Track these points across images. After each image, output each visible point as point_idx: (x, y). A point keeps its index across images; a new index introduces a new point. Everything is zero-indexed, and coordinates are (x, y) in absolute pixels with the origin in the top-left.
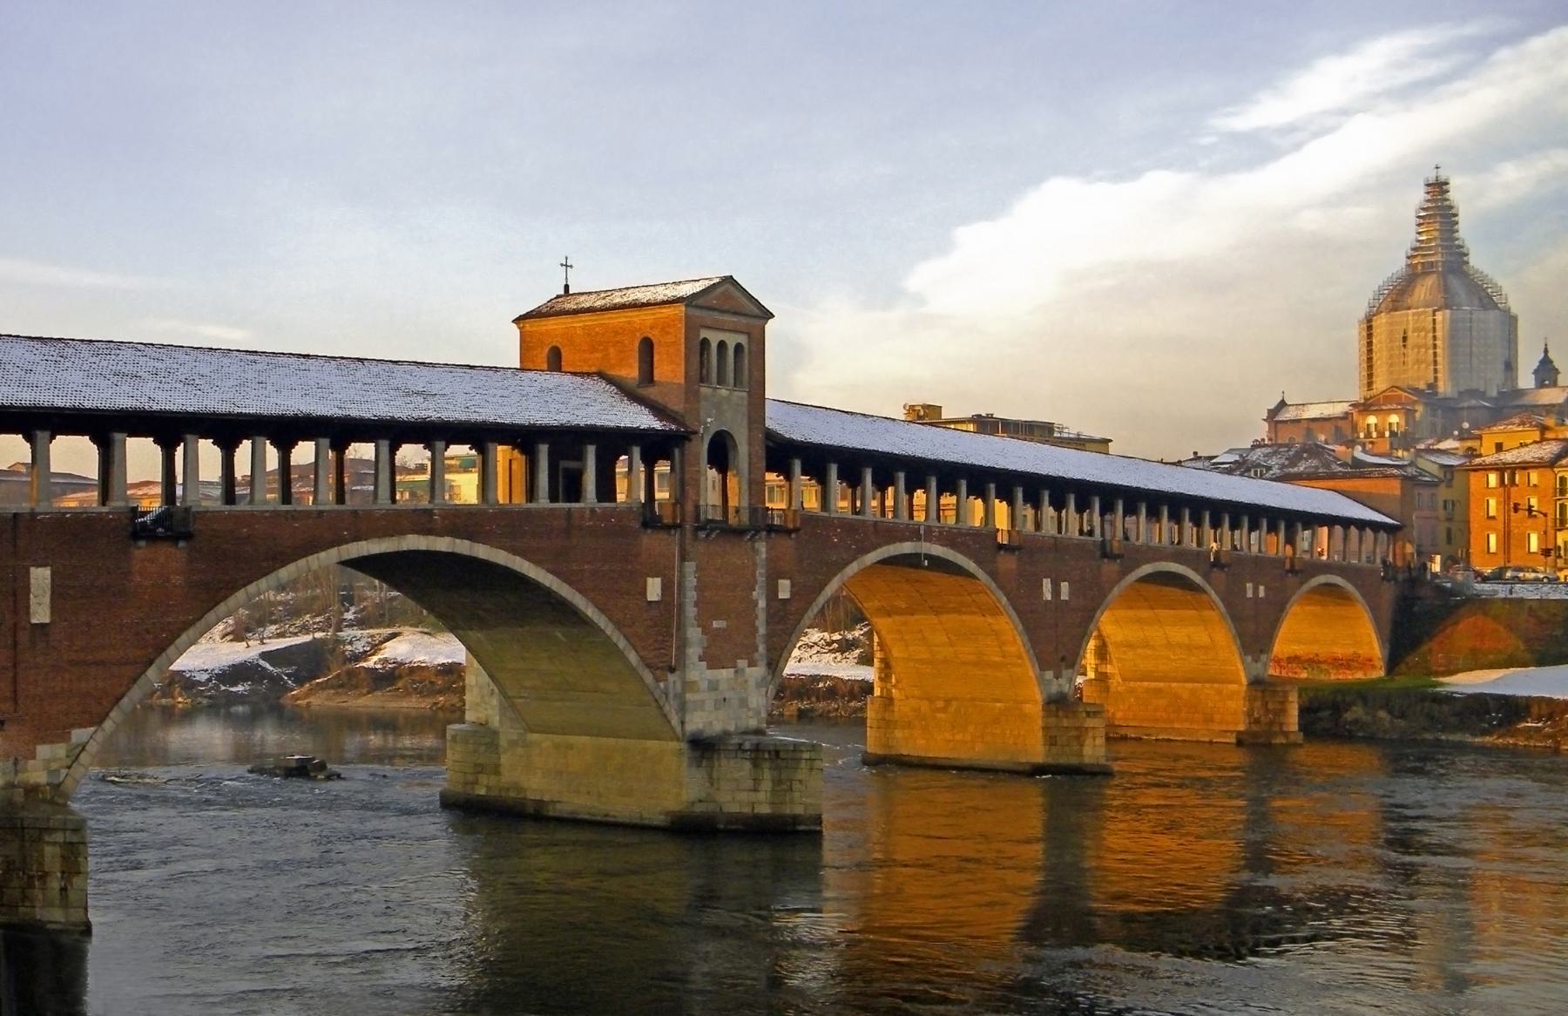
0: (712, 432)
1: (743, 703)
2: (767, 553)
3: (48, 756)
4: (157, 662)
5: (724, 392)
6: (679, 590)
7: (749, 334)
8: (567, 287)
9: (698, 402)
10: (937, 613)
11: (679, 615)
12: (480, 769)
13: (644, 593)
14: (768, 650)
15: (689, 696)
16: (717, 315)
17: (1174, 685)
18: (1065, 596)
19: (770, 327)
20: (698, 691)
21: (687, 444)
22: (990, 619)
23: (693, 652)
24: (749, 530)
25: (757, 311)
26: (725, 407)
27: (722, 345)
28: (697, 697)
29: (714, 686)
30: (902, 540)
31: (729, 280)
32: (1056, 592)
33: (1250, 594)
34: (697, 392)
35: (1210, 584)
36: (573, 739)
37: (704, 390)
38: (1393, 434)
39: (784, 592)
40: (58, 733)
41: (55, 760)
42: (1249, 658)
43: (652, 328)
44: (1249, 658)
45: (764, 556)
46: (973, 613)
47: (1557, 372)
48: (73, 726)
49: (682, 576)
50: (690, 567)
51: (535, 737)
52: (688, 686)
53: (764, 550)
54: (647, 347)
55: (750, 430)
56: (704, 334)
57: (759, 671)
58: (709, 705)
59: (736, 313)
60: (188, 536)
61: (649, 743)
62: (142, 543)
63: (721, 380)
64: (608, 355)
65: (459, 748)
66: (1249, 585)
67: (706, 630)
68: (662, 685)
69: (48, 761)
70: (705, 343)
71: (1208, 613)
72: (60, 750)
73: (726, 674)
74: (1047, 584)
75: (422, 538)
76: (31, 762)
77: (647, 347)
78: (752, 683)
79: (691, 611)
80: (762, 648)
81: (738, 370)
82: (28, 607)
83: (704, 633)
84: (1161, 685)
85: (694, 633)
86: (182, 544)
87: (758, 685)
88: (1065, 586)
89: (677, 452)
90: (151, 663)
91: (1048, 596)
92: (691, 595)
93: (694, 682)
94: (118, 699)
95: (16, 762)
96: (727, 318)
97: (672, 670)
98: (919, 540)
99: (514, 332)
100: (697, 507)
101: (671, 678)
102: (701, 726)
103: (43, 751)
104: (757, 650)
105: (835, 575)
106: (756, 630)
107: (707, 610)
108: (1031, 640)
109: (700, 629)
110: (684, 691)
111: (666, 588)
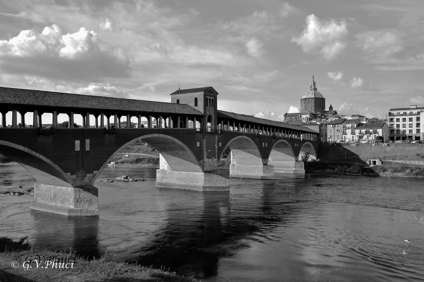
0: (208, 115)
1: (213, 165)
2: (218, 137)
3: (89, 176)
4: (110, 158)
5: (210, 108)
6: (203, 144)
7: (214, 97)
8: (179, 88)
9: (206, 109)
10: (244, 149)
11: (202, 149)
12: (163, 178)
13: (196, 145)
14: (218, 155)
15: (204, 164)
16: (209, 94)
17: (282, 162)
18: (266, 146)
19: (218, 96)
20: (206, 163)
21: (204, 117)
22: (254, 150)
23: (205, 156)
24: (214, 134)
25: (216, 93)
26: (210, 111)
27: (210, 99)
28: (206, 164)
29: (208, 162)
30: (240, 136)
31: (212, 87)
32: (265, 145)
33: (295, 145)
34: (206, 108)
35: (289, 143)
36: (181, 172)
37: (207, 107)
38: (308, 118)
39: (220, 145)
41: (90, 177)
42: (295, 157)
43: (197, 96)
44: (295, 157)
45: (217, 138)
46: (251, 149)
47: (333, 108)
48: (94, 170)
49: (203, 142)
50: (204, 140)
51: (174, 172)
52: (204, 162)
53: (217, 137)
54: (196, 99)
55: (215, 115)
56: (207, 97)
57: (216, 159)
58: (208, 166)
59: (212, 93)
60: (115, 134)
61: (196, 173)
62: (107, 135)
64: (188, 101)
65: (159, 174)
66: (295, 144)
67: (207, 152)
68: (200, 162)
69: (89, 177)
70: (207, 99)
71: (289, 149)
72: (91, 175)
73: (210, 160)
74: (263, 143)
75: (158, 134)
76: (86, 178)
77: (196, 99)
78: (215, 161)
79: (205, 148)
80: (217, 155)
81: (212, 104)
82: (85, 147)
83: (207, 152)
84: (279, 162)
85: (205, 152)
86: (114, 135)
87: (216, 162)
88: (266, 144)
89: (202, 119)
90: (108, 158)
91: (264, 146)
92: (205, 145)
93: (205, 162)
94: (102, 165)
95: (83, 178)
96: (211, 94)
97: (201, 159)
98: (243, 135)
99: (170, 97)
100: (206, 129)
101: (201, 161)
102: (206, 170)
103: (88, 175)
104: (216, 155)
105: (229, 142)
106: (216, 152)
107: (207, 148)
108: (261, 153)
110: (203, 163)
111: (200, 144)
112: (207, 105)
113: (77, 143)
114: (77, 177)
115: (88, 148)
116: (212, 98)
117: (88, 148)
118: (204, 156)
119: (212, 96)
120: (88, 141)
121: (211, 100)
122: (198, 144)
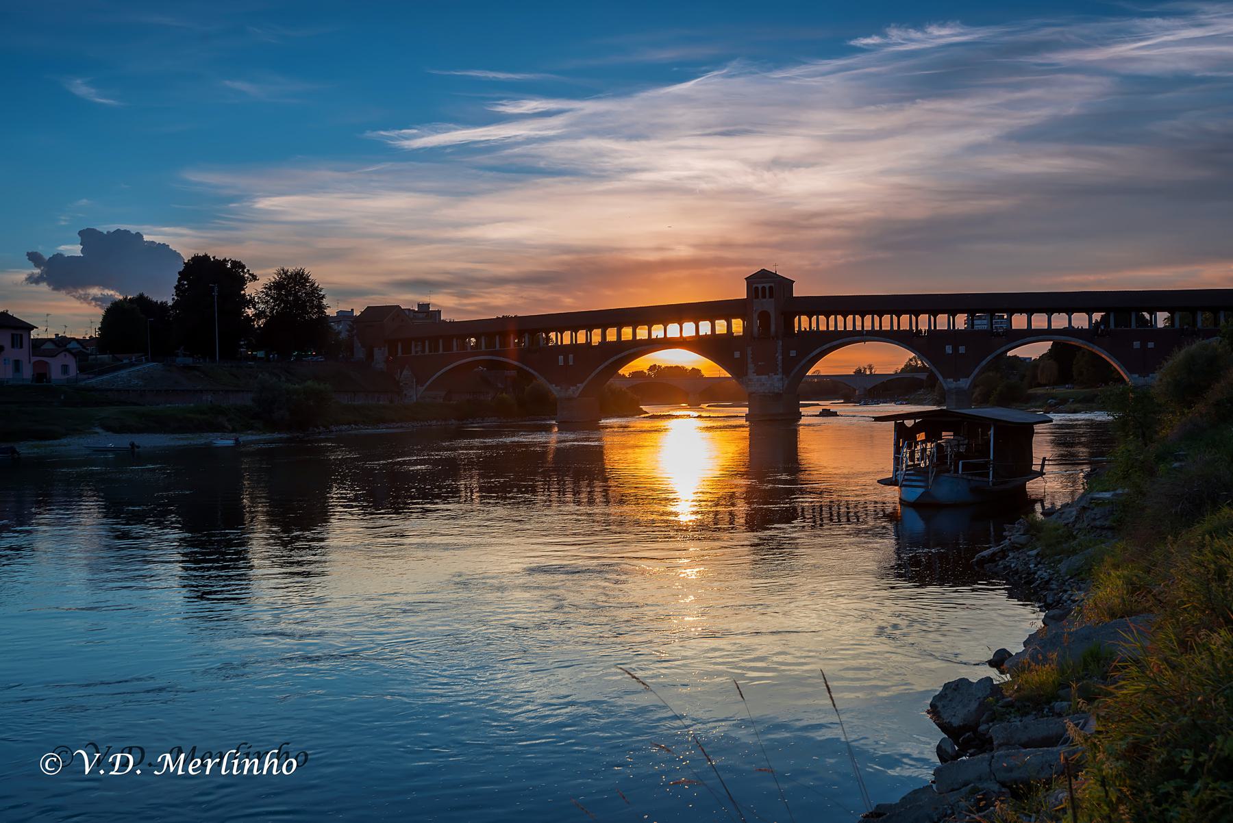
5: (764, 300)
27: (764, 288)
32: (955, 349)
45: (781, 344)
56: (756, 285)
57: (780, 376)
63: (764, 297)
72: (575, 388)
79: (750, 360)
80: (780, 370)
103: (572, 388)
109: (753, 365)
112: (757, 297)
113: (561, 358)
114: (561, 389)
115: (571, 363)
117: (571, 363)
120: (571, 356)
121: (760, 288)
122: (737, 355)
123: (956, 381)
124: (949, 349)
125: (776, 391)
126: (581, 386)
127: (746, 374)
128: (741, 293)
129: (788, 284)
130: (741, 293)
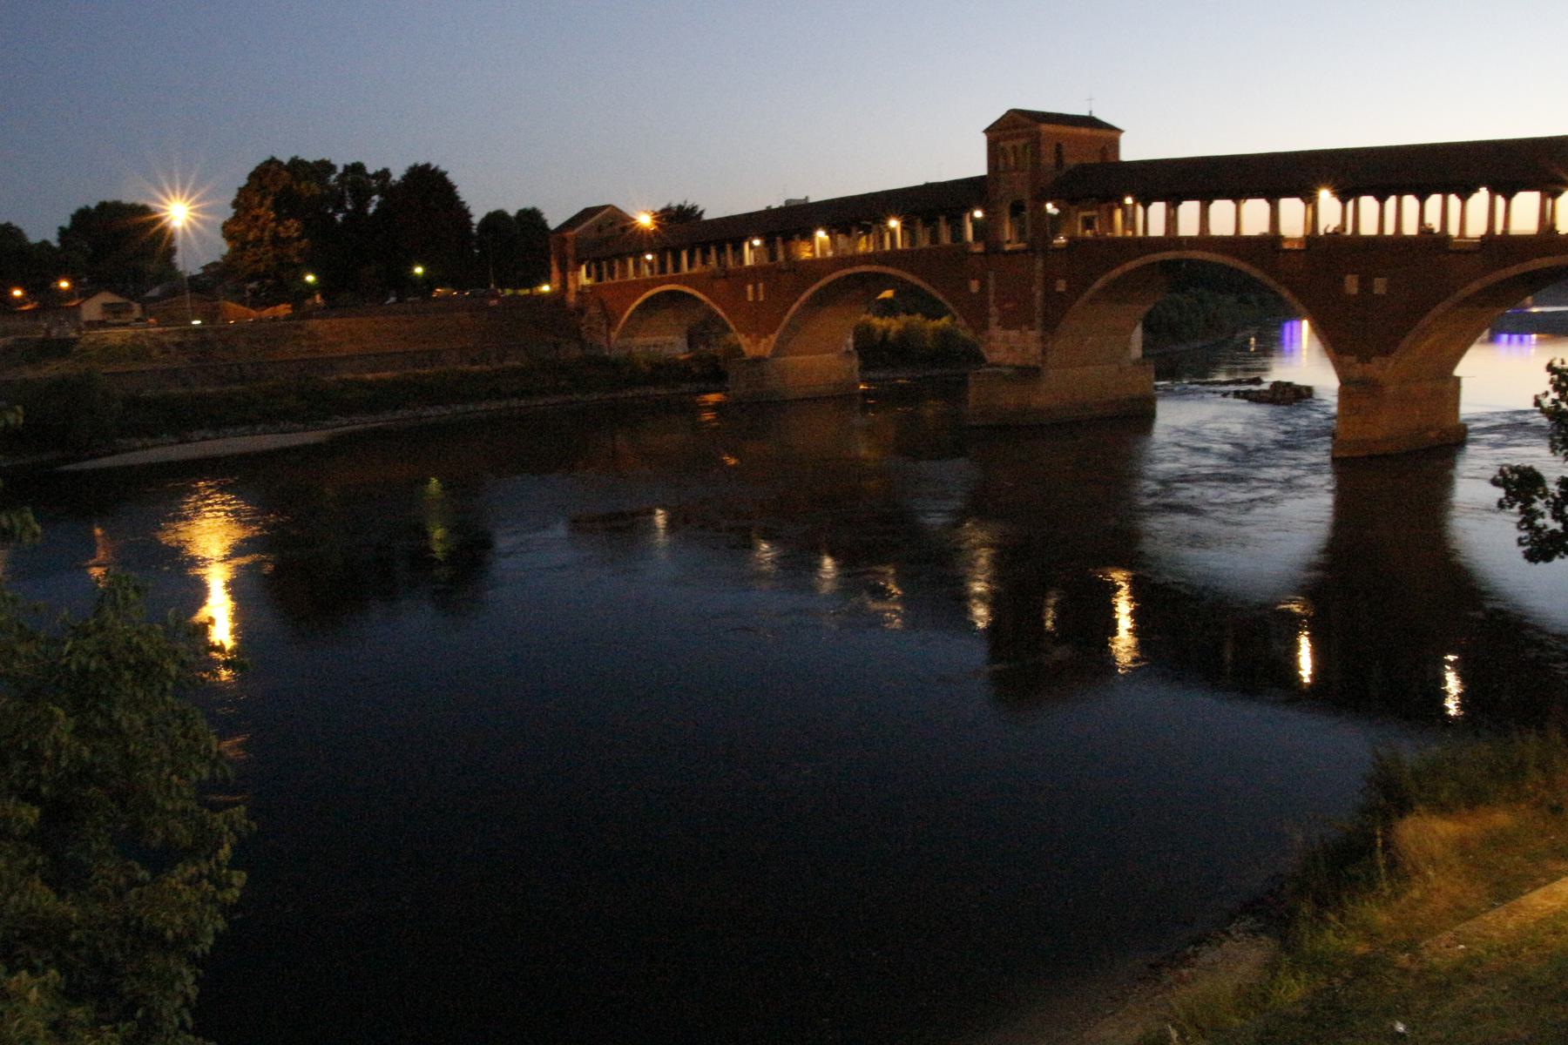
1: (1025, 350)
8: (1091, 112)
13: (968, 288)
23: (993, 320)
27: (1014, 147)
31: (1009, 112)
32: (1365, 284)
40: (766, 335)
50: (991, 275)
52: (990, 338)
73: (1013, 333)
80: (1039, 321)
85: (993, 309)
92: (992, 289)
103: (764, 341)
104: (1034, 321)
113: (750, 288)
115: (761, 298)
116: (1021, 142)
117: (761, 298)
118: (991, 320)
119: (1018, 136)
120: (761, 285)
122: (974, 286)
123: (1363, 363)
124: (1352, 285)
125: (1032, 363)
126: (773, 338)
127: (986, 327)
128: (974, 163)
129: (1110, 134)
130: (974, 163)
